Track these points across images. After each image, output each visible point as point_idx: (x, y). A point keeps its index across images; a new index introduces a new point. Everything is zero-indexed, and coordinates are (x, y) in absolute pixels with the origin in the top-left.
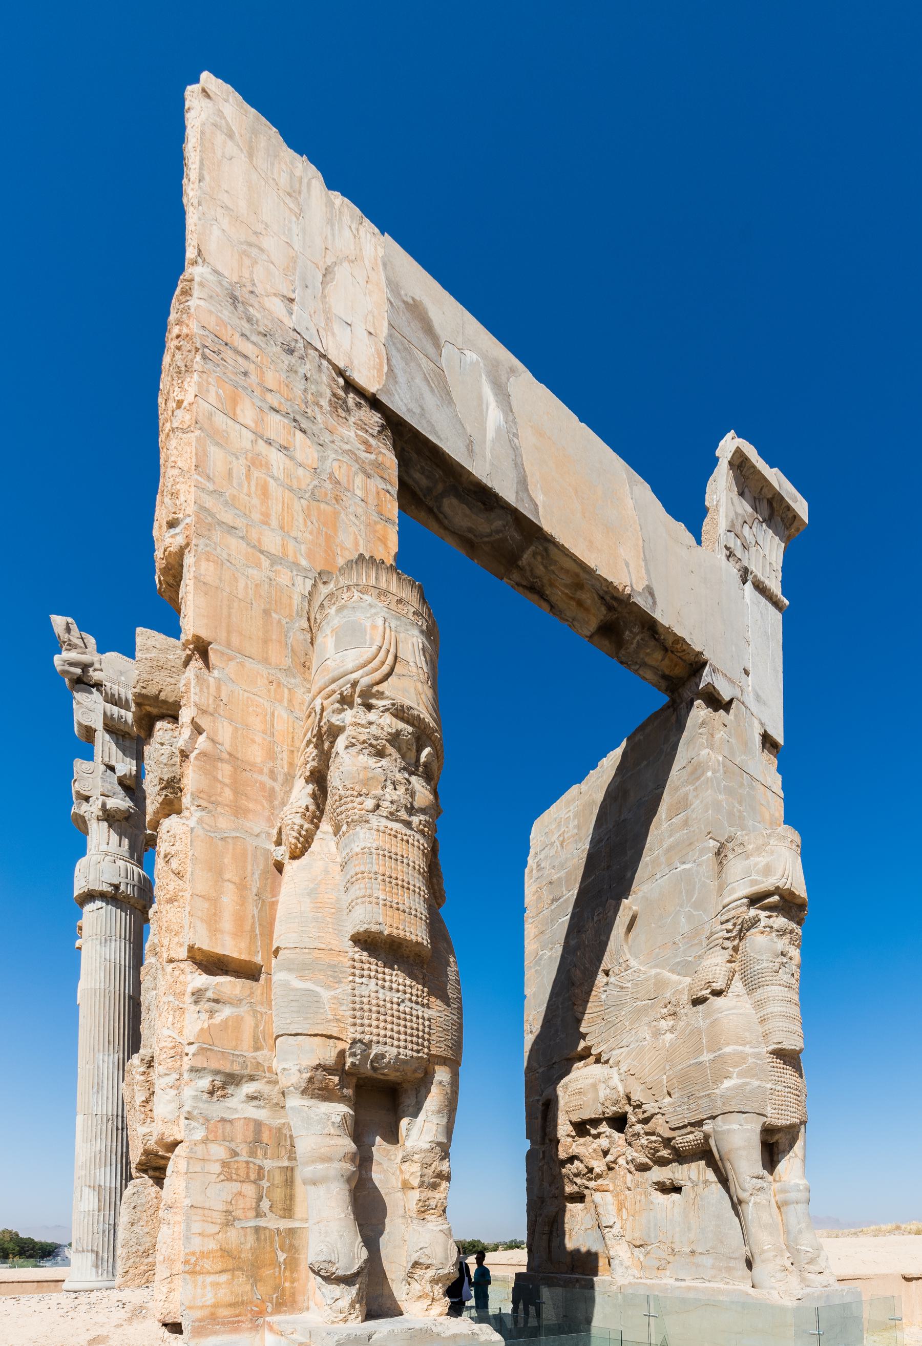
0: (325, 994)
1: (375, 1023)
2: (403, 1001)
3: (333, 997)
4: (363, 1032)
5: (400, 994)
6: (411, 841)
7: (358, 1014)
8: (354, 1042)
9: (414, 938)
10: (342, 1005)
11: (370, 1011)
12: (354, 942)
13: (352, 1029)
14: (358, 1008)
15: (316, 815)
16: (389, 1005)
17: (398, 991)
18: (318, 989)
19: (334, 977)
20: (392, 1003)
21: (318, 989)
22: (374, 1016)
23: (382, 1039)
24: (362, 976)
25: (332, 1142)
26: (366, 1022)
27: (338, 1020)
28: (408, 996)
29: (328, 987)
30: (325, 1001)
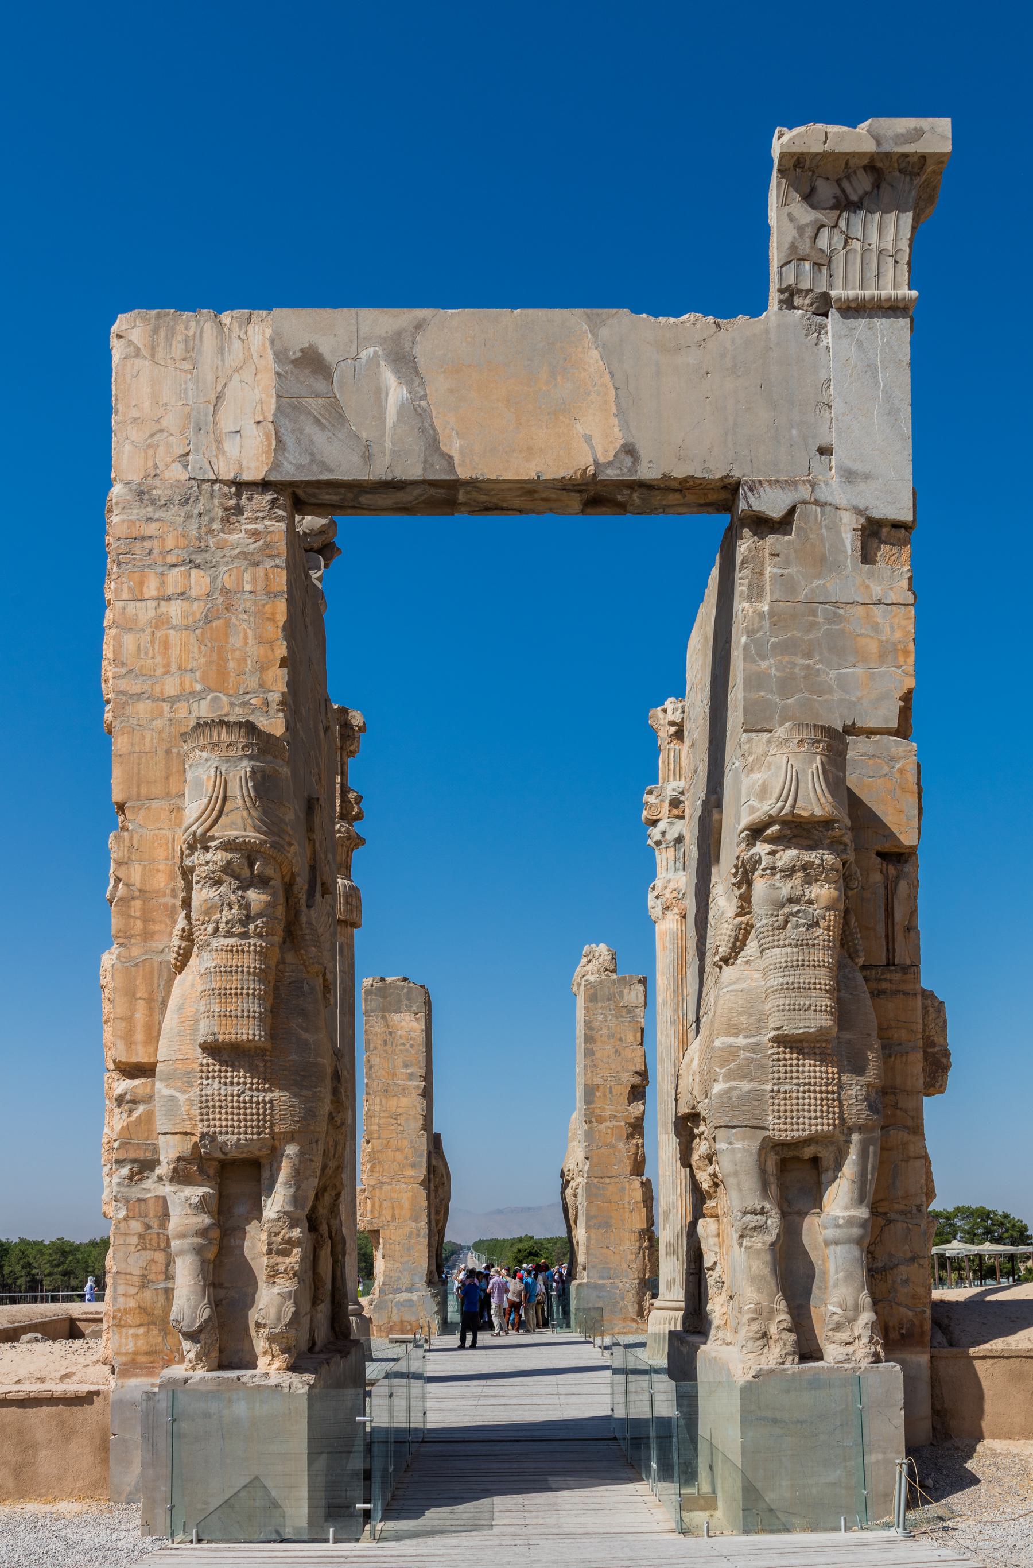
0: (182, 1098)
1: (218, 1116)
2: (243, 1092)
3: (187, 1100)
4: (209, 1126)
5: (239, 1087)
6: (246, 949)
7: (204, 1111)
8: (203, 1136)
9: (244, 1037)
10: (193, 1105)
11: (214, 1107)
12: (203, 1049)
13: (200, 1126)
14: (206, 1106)
15: (188, 936)
16: (229, 1099)
17: (238, 1084)
18: (178, 1094)
19: (188, 1082)
20: (233, 1096)
21: (178, 1094)
22: (217, 1110)
23: (224, 1129)
24: (208, 1078)
25: (187, 1222)
26: (211, 1117)
27: (190, 1119)
28: (248, 1086)
29: (183, 1092)
30: (181, 1103)
